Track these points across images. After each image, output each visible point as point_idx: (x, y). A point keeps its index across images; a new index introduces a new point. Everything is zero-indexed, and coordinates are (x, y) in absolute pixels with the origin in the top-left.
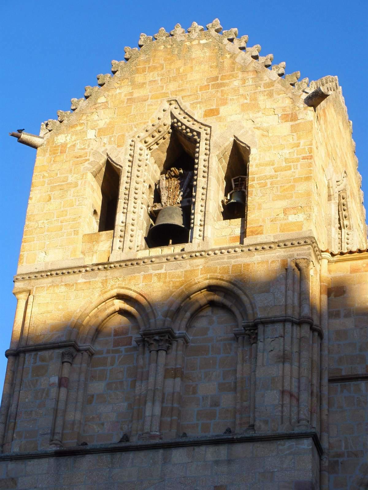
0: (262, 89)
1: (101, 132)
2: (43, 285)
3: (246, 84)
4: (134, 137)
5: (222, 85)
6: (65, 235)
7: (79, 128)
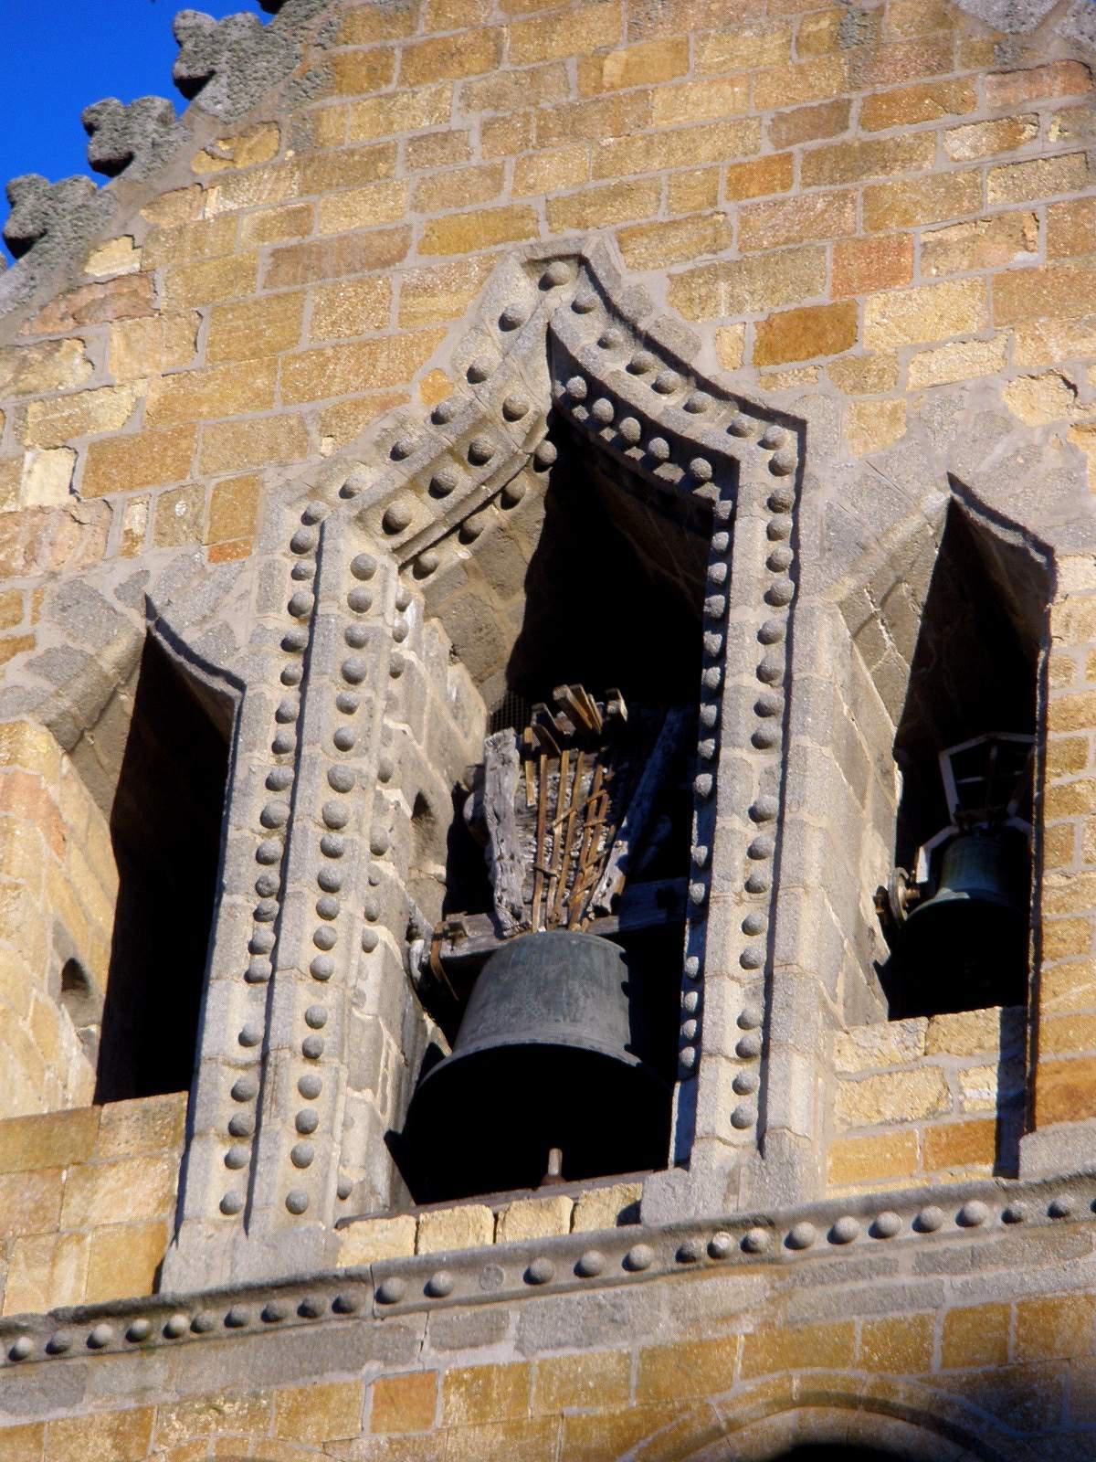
3: (1024, 151)
4: (315, 492)
5: (873, 156)
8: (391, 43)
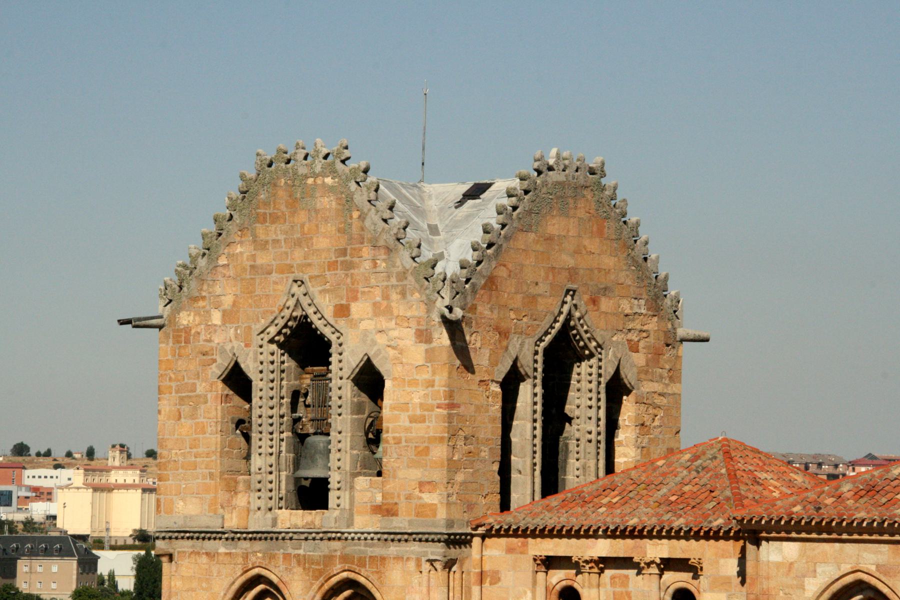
0: (394, 281)
1: (227, 317)
2: (184, 550)
3: (378, 270)
6: (200, 478)
7: (201, 303)
8: (267, 211)
